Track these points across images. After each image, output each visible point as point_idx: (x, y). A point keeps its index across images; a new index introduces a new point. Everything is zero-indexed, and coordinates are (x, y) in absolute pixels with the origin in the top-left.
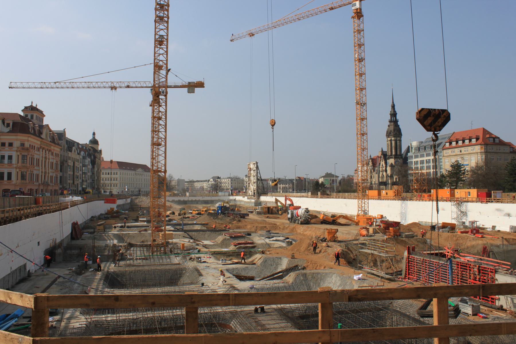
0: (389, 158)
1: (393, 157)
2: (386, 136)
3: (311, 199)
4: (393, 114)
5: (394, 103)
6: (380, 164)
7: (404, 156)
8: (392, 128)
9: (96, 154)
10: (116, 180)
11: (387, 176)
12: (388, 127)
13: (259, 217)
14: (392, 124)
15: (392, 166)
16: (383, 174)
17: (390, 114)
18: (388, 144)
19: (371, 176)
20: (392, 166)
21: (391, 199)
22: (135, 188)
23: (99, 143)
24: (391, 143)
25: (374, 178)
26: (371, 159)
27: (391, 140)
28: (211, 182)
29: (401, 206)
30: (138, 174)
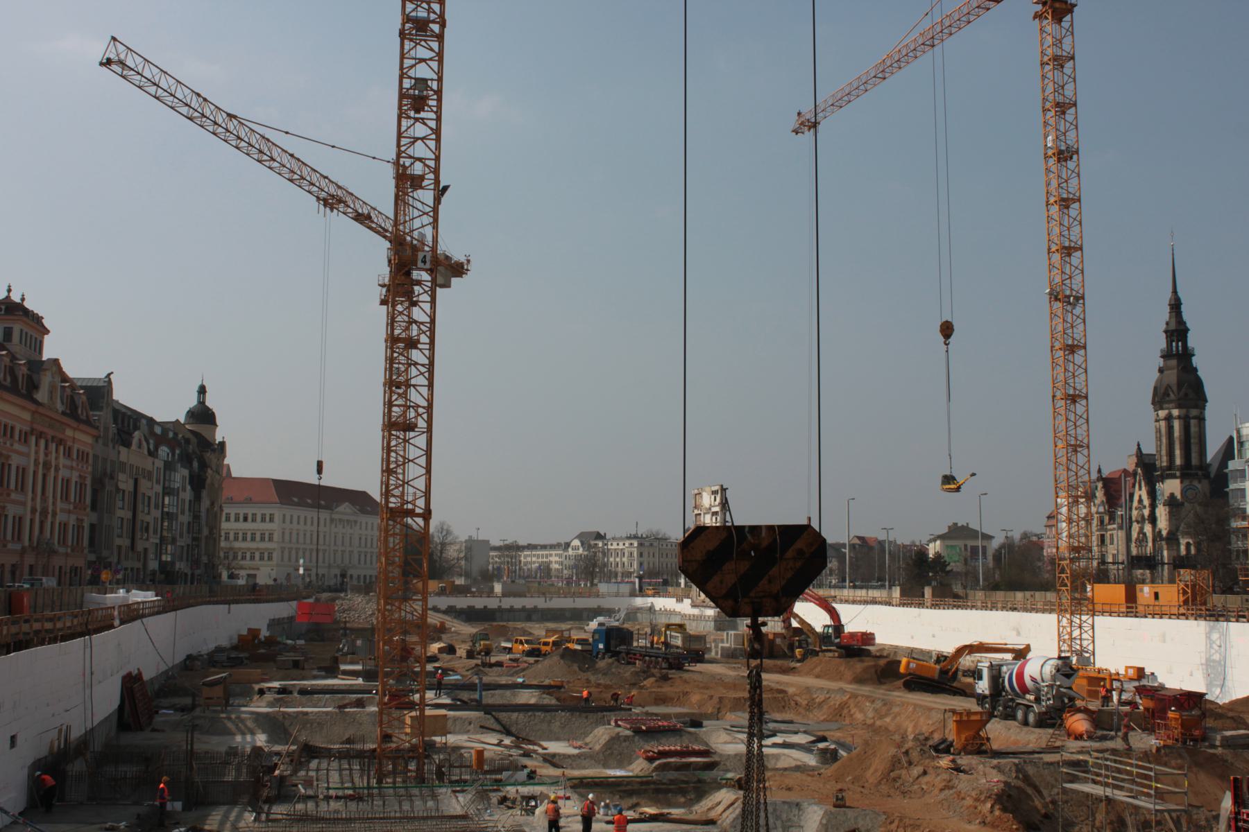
0: (1162, 478)
1: (1178, 473)
2: (1153, 403)
3: (901, 609)
4: (1176, 330)
5: (1180, 294)
6: (1132, 495)
7: (1213, 471)
8: (1172, 377)
9: (209, 455)
10: (271, 539)
11: (1157, 536)
12: (1157, 375)
13: (730, 668)
14: (1174, 362)
15: (1172, 502)
16: (1141, 531)
17: (1166, 332)
18: (1158, 431)
19: (1102, 536)
20: (1172, 502)
21: (1170, 616)
22: (330, 566)
23: (218, 421)
24: (1170, 429)
25: (1112, 543)
26: (1100, 478)
27: (1169, 418)
28: (576, 548)
29: (1208, 637)
30: (340, 520)
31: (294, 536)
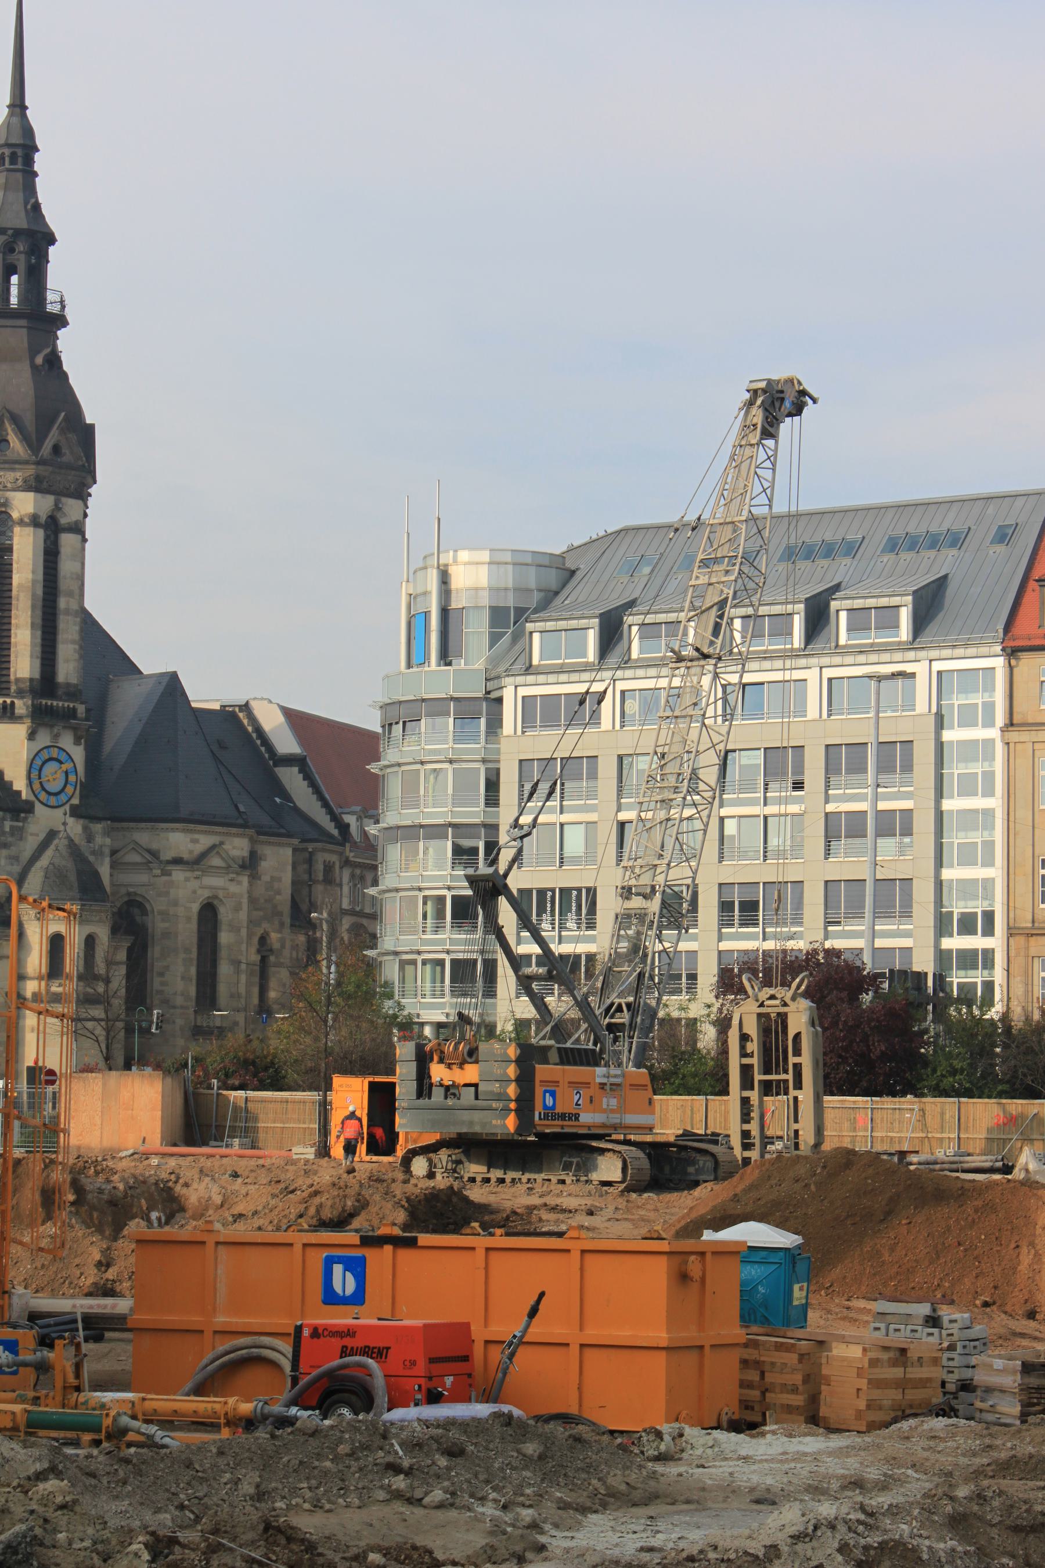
1: (21, 706)
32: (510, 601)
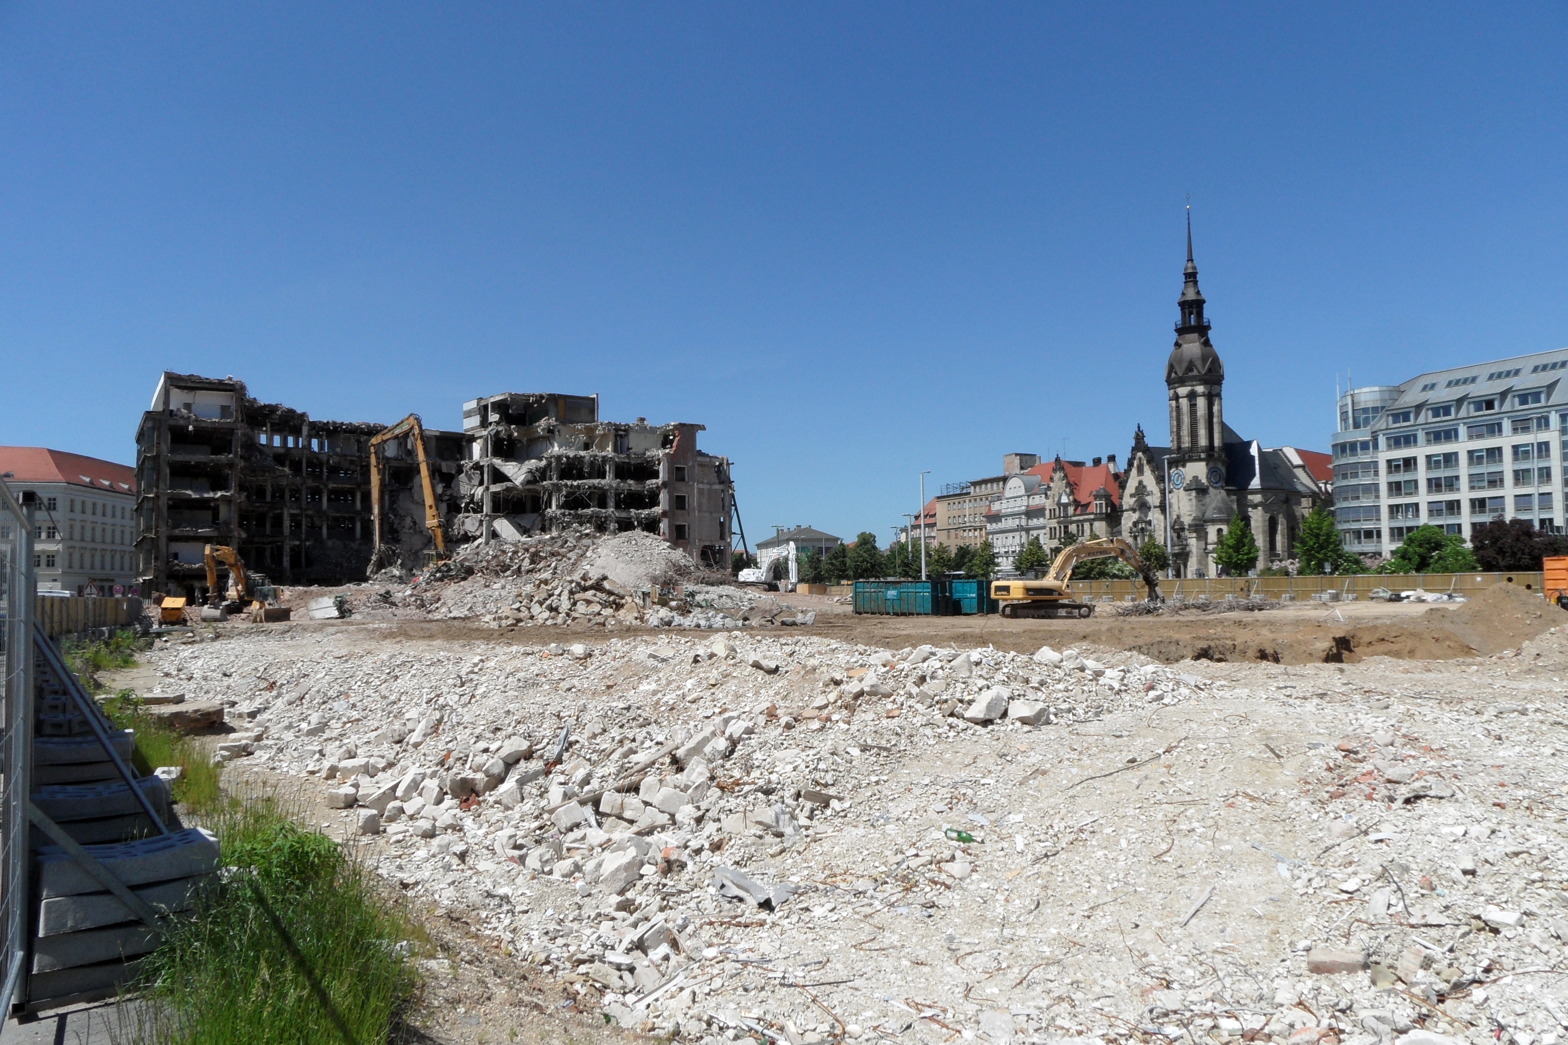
1: (1203, 456)
12: (1172, 348)
31: (98, 534)
32: (1379, 404)
